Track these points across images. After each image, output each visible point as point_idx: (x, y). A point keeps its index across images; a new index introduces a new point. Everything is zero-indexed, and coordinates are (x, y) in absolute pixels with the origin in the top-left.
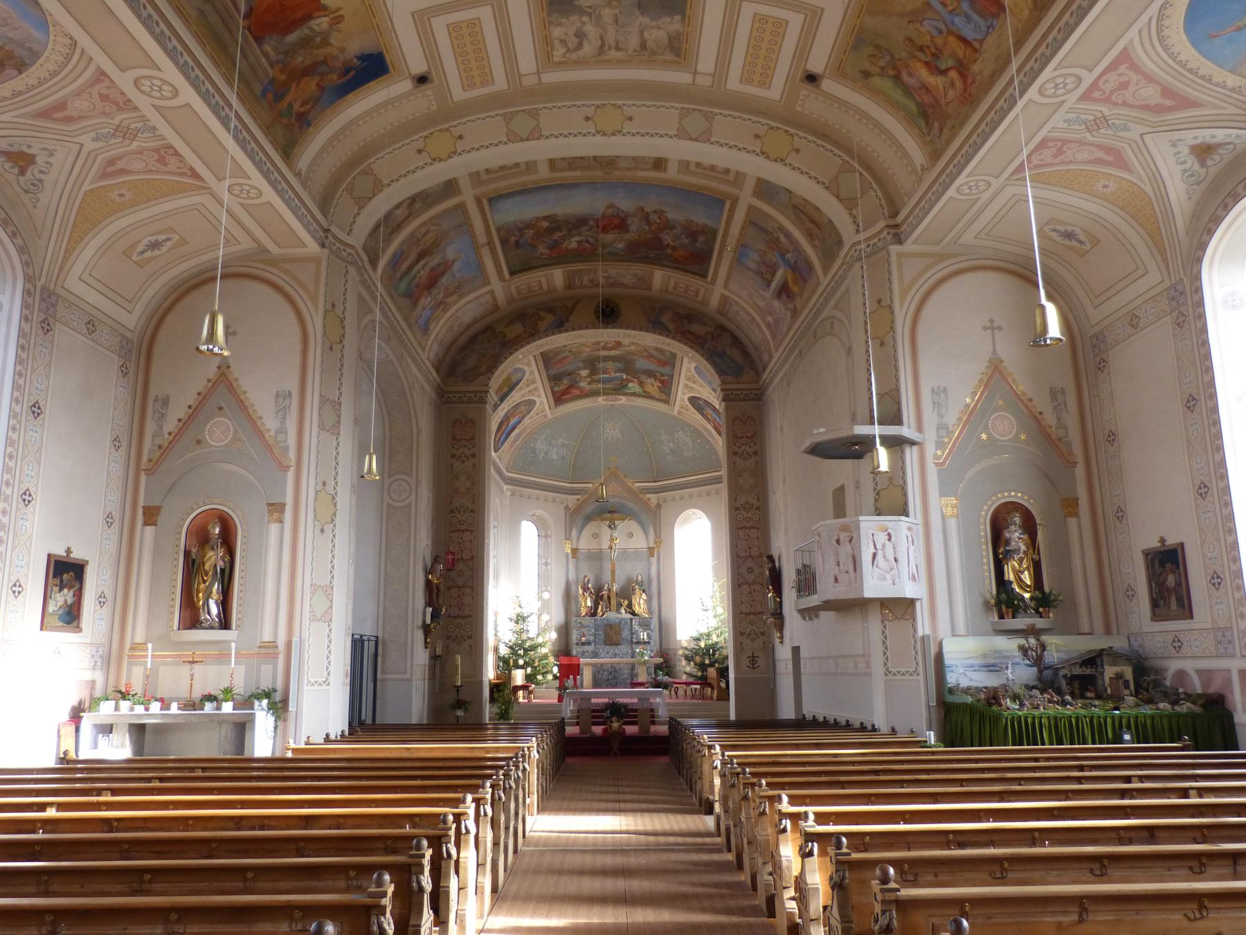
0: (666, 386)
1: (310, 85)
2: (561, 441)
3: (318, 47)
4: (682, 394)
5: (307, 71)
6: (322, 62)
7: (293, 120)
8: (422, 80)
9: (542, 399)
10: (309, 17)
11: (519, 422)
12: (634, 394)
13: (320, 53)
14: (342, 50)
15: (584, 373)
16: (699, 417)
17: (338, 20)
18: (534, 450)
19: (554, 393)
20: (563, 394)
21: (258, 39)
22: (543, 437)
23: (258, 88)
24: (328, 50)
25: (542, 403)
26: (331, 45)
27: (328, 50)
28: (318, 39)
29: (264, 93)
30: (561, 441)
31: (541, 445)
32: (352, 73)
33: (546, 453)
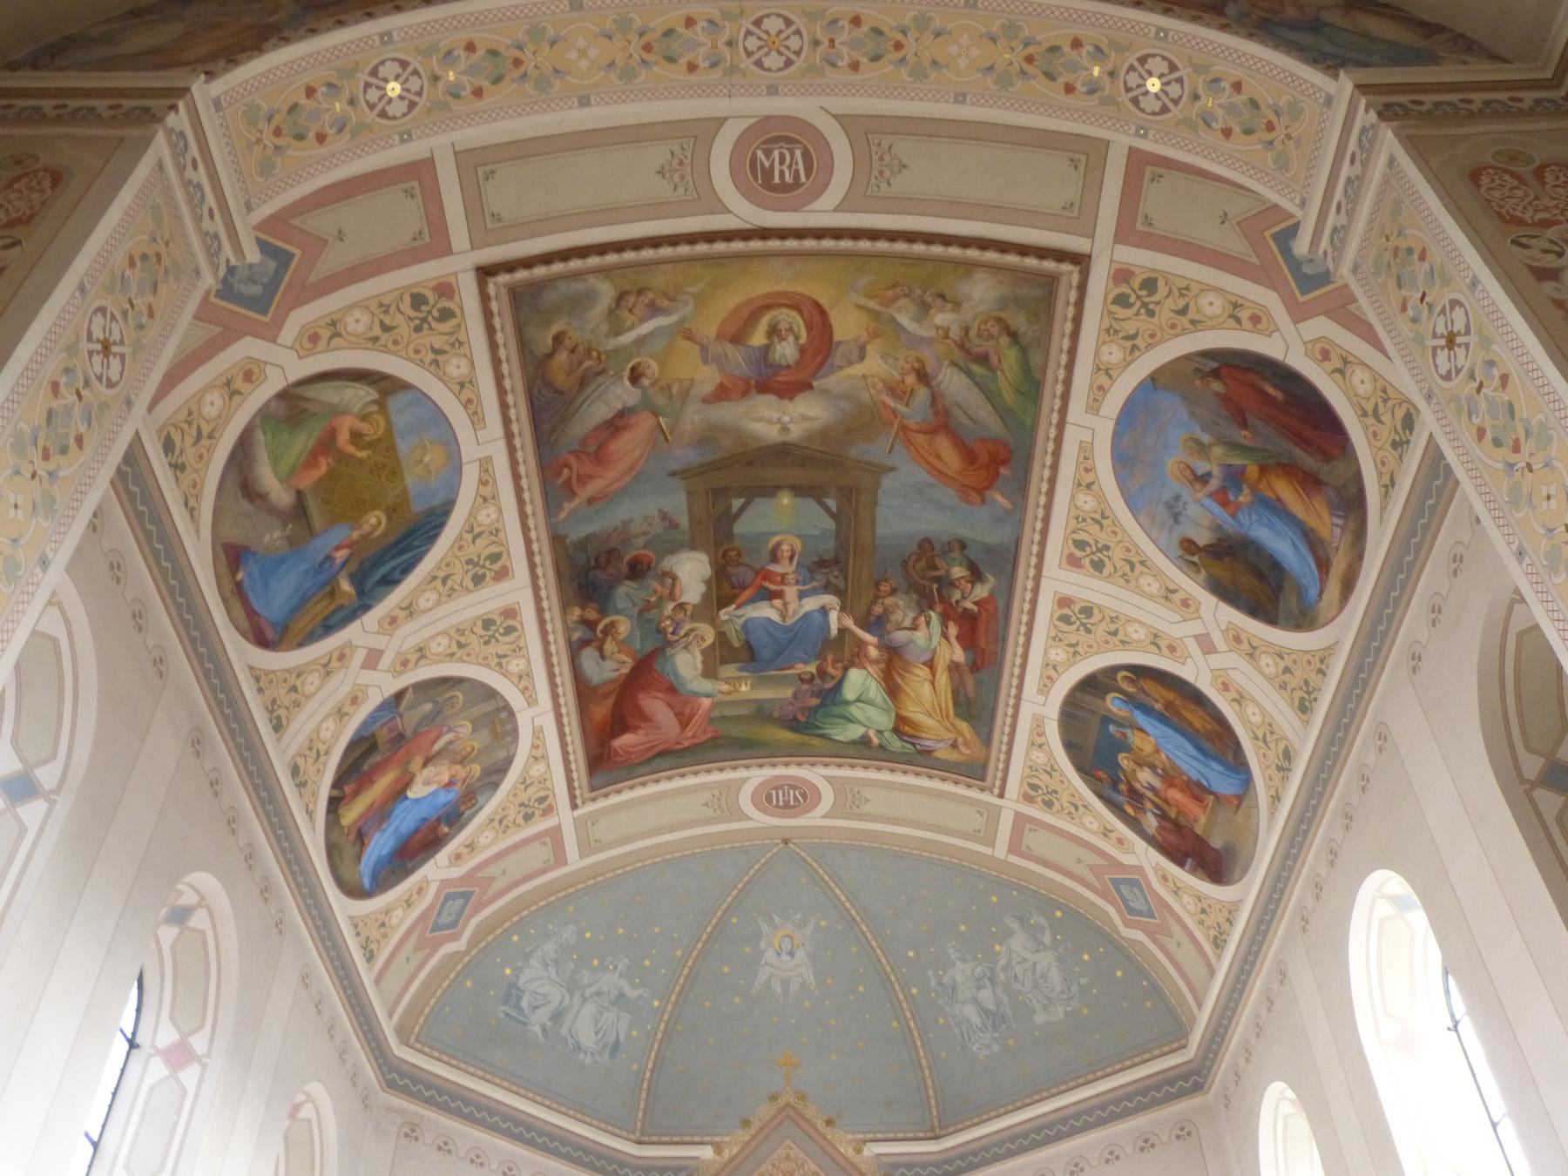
0: (983, 639)
2: (610, 981)
4: (1041, 682)
9: (543, 727)
11: (453, 818)
12: (865, 750)
15: (692, 572)
16: (1096, 820)
18: (512, 994)
19: (585, 692)
20: (621, 721)
22: (549, 948)
25: (538, 733)
30: (610, 981)
31: (539, 981)
33: (557, 1017)
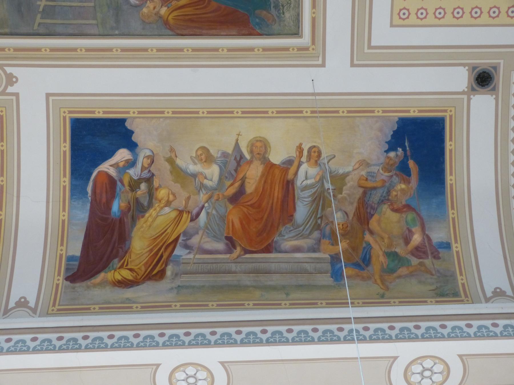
1: (387, 220)
3: (339, 190)
5: (364, 215)
6: (365, 193)
7: (415, 261)
8: (483, 79)
10: (289, 186)
13: (351, 189)
14: (364, 163)
17: (315, 155)
21: (268, 250)
23: (327, 279)
24: (351, 182)
26: (346, 175)
27: (351, 182)
28: (328, 185)
29: (337, 275)
32: (411, 164)
